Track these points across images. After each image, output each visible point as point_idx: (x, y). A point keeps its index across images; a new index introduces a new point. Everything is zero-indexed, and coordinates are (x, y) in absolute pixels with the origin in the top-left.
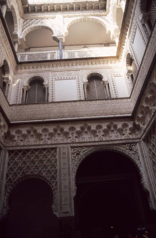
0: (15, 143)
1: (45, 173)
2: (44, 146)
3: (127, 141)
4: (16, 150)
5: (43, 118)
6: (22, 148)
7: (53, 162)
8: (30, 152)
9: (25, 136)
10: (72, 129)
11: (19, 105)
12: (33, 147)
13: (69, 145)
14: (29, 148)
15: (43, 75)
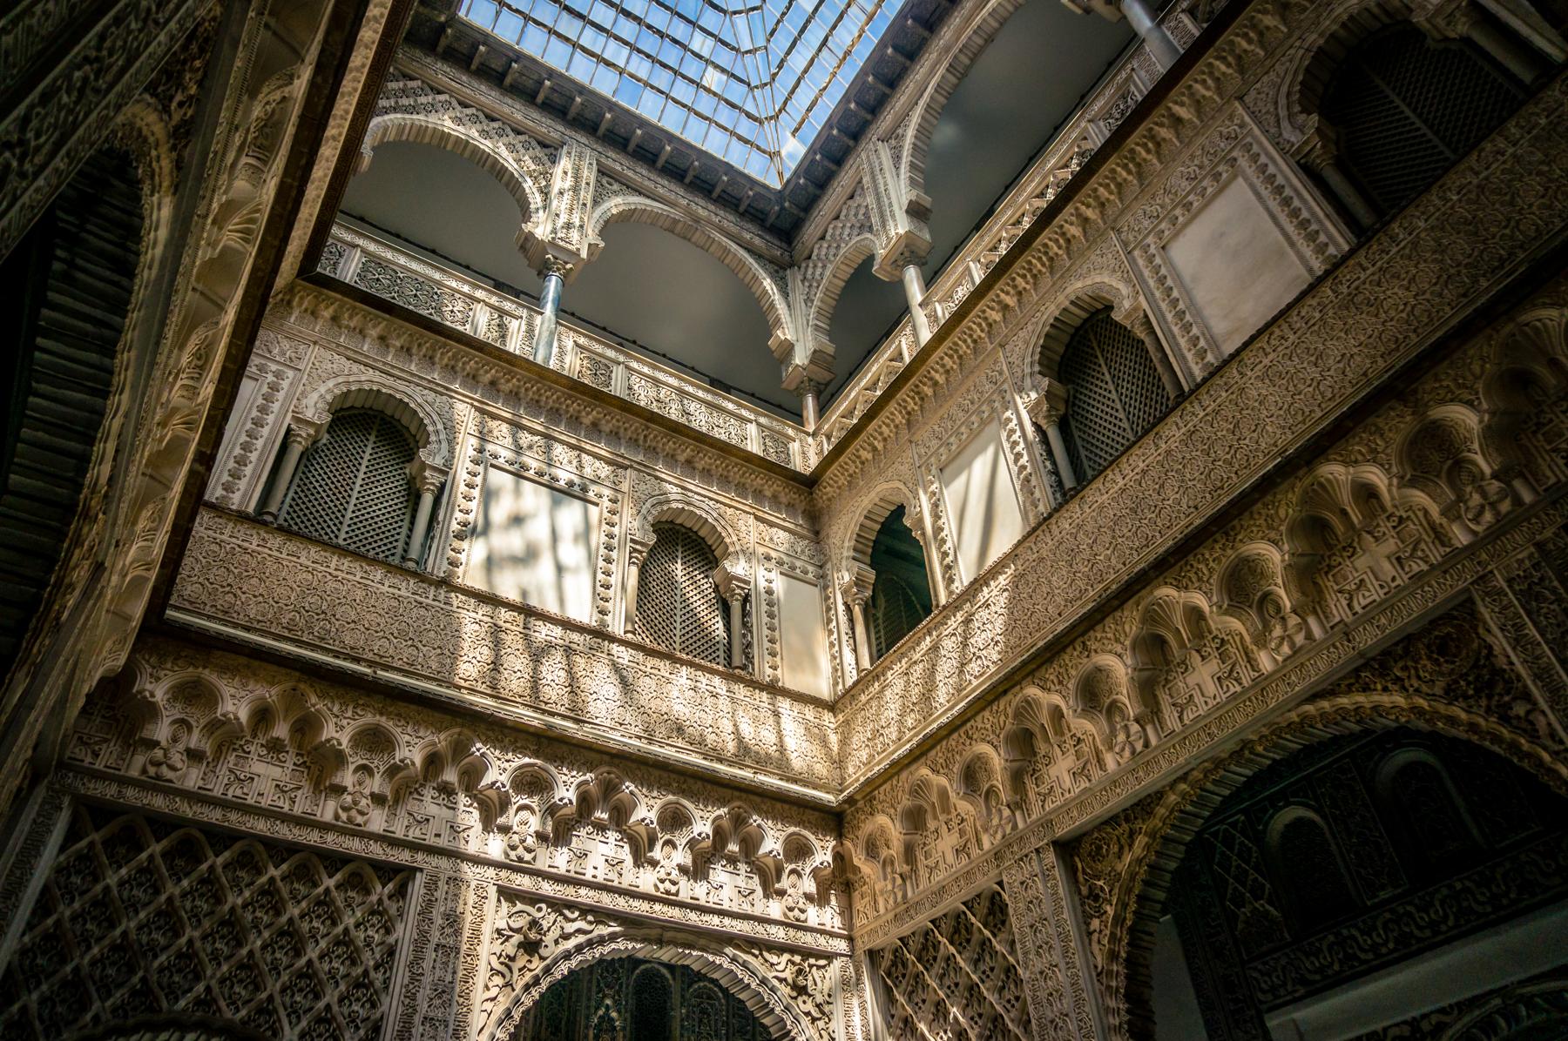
0: (140, 760)
1: (297, 1030)
2: (341, 839)
3: (792, 932)
4: (135, 809)
5: (370, 656)
6: (187, 810)
7: (372, 963)
8: (227, 854)
9: (227, 738)
10: (531, 783)
11: (241, 517)
12: (261, 826)
13: (491, 872)
14: (235, 820)
15: (428, 409)
